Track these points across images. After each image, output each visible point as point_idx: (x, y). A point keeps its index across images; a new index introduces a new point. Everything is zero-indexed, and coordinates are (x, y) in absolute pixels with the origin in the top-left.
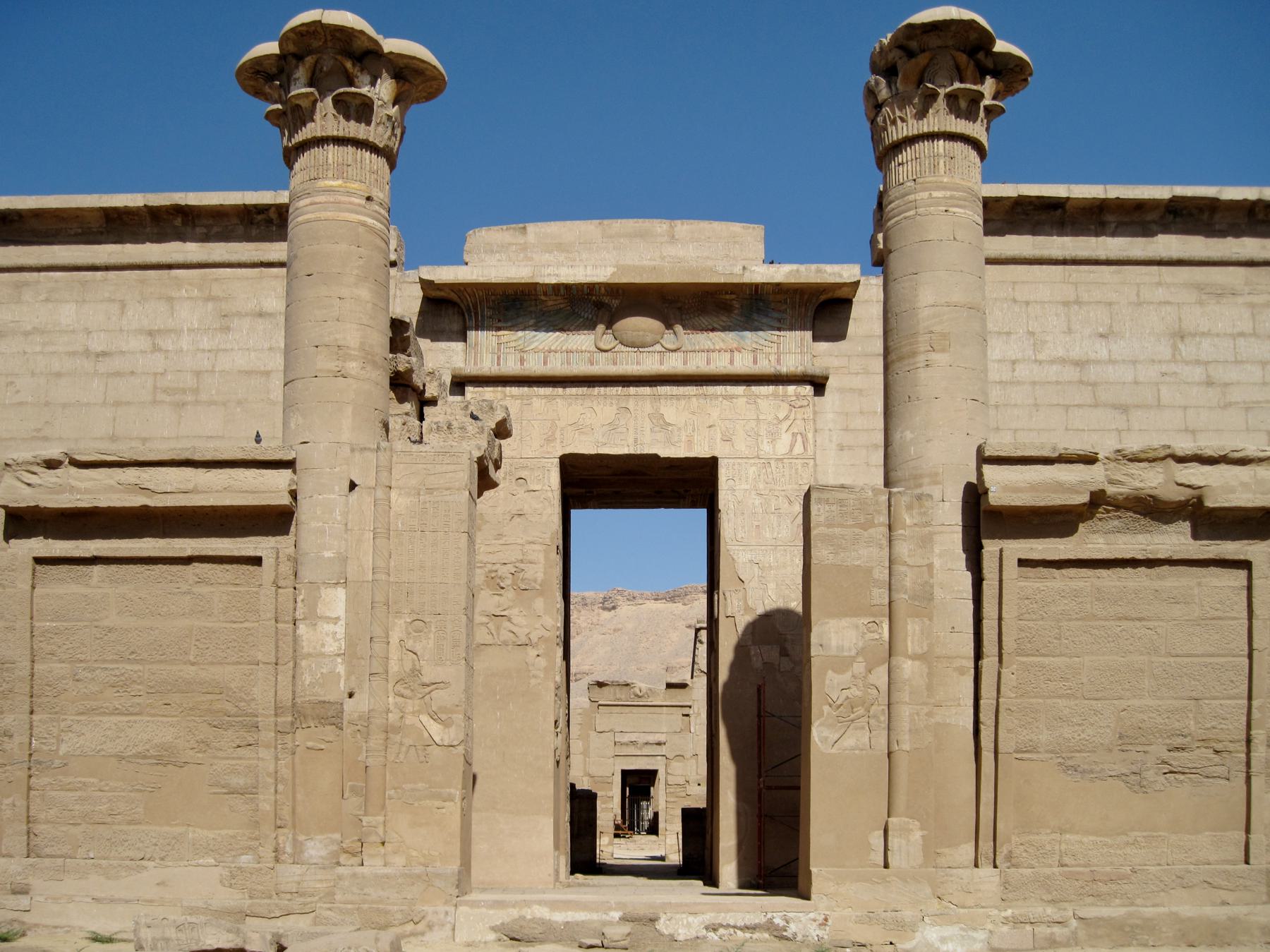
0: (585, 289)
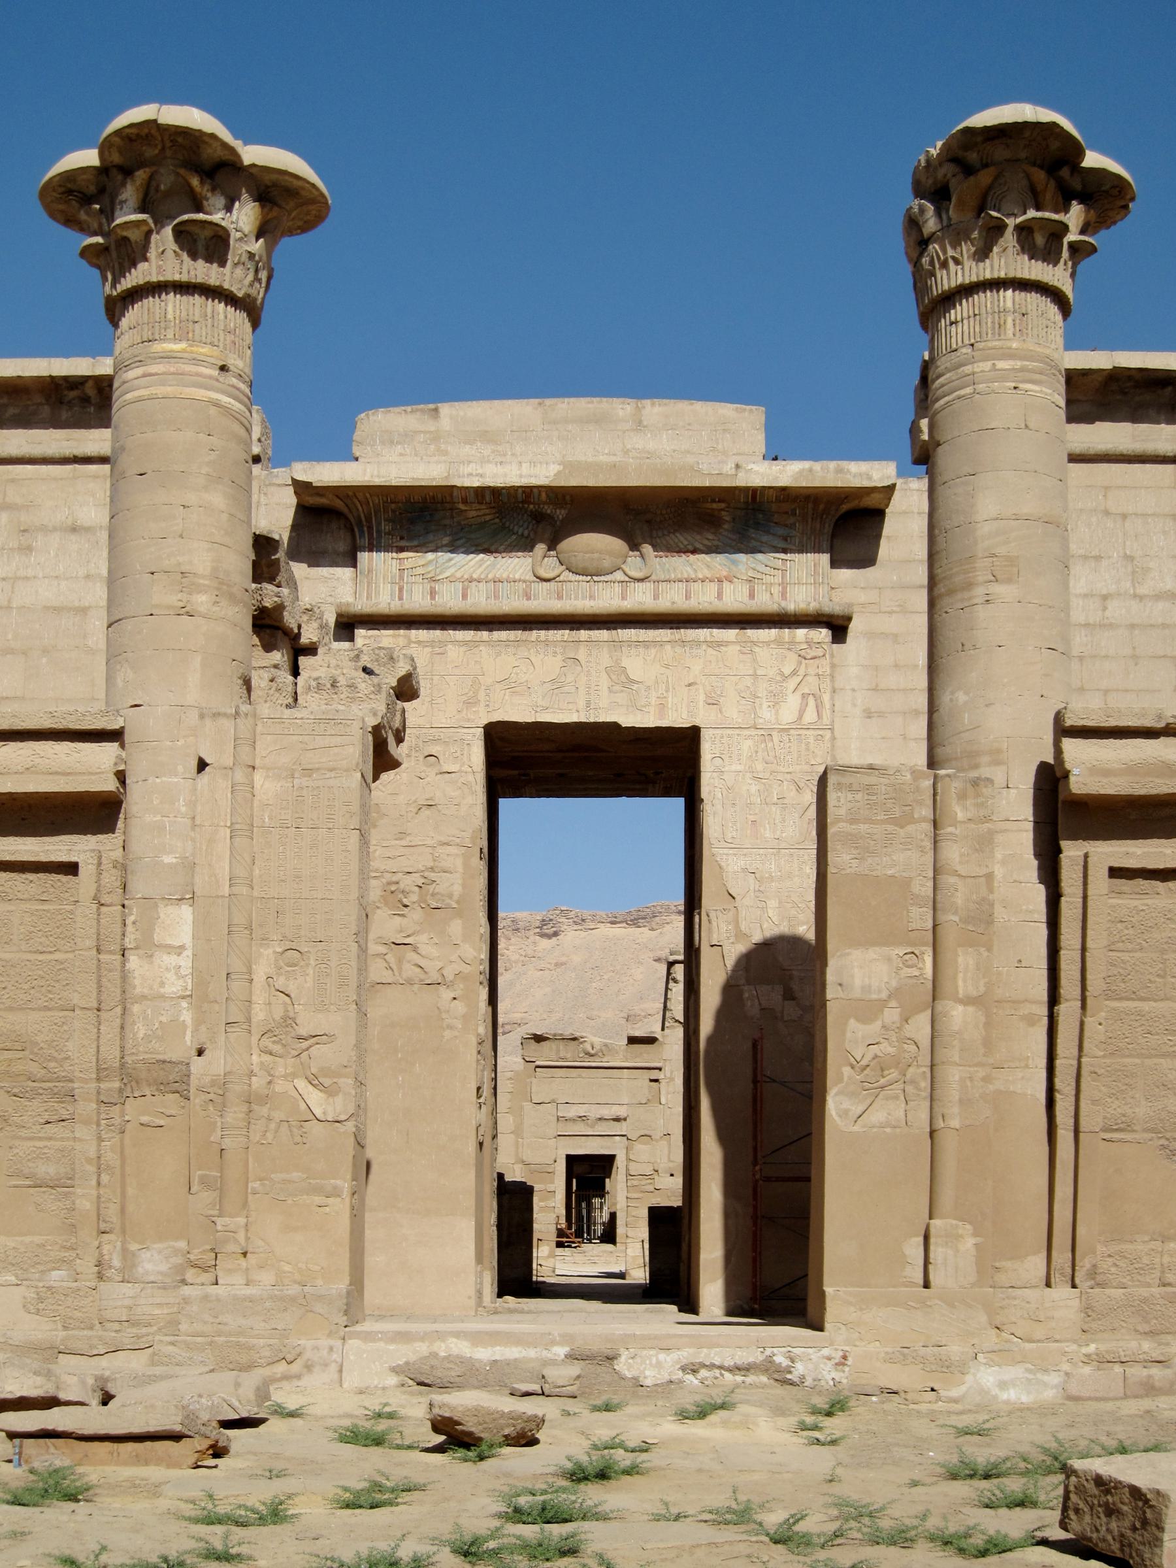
0: (520, 496)
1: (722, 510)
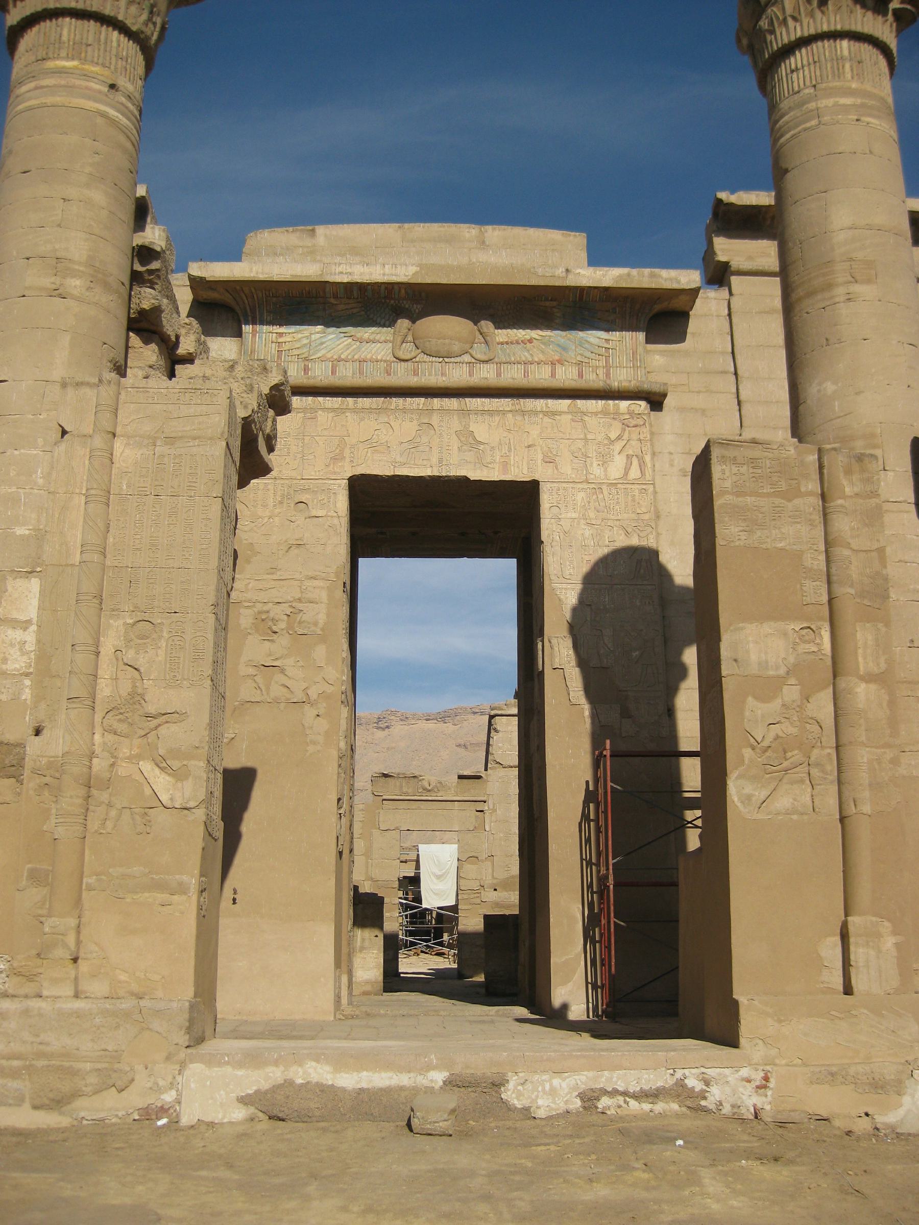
1: (554, 307)
